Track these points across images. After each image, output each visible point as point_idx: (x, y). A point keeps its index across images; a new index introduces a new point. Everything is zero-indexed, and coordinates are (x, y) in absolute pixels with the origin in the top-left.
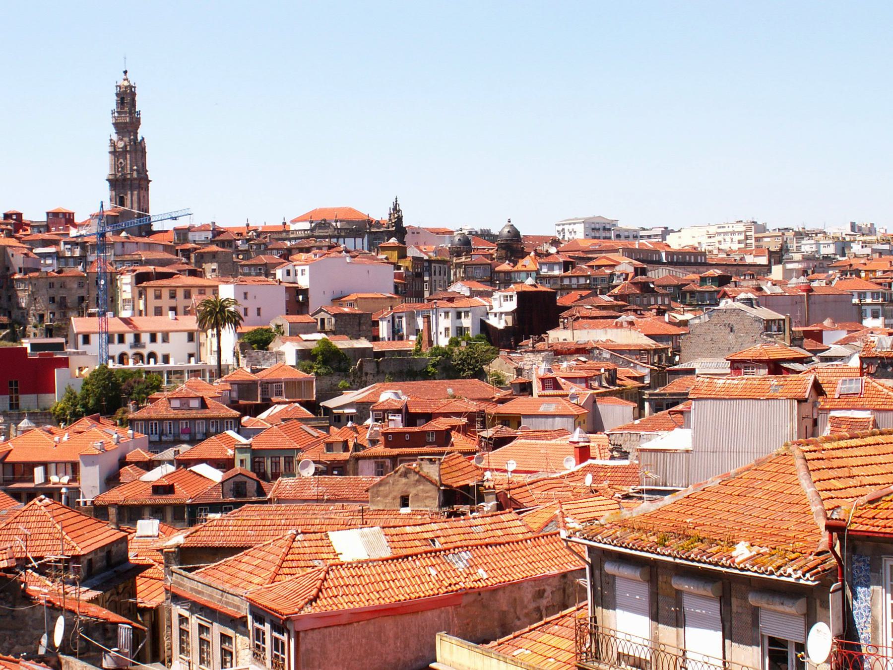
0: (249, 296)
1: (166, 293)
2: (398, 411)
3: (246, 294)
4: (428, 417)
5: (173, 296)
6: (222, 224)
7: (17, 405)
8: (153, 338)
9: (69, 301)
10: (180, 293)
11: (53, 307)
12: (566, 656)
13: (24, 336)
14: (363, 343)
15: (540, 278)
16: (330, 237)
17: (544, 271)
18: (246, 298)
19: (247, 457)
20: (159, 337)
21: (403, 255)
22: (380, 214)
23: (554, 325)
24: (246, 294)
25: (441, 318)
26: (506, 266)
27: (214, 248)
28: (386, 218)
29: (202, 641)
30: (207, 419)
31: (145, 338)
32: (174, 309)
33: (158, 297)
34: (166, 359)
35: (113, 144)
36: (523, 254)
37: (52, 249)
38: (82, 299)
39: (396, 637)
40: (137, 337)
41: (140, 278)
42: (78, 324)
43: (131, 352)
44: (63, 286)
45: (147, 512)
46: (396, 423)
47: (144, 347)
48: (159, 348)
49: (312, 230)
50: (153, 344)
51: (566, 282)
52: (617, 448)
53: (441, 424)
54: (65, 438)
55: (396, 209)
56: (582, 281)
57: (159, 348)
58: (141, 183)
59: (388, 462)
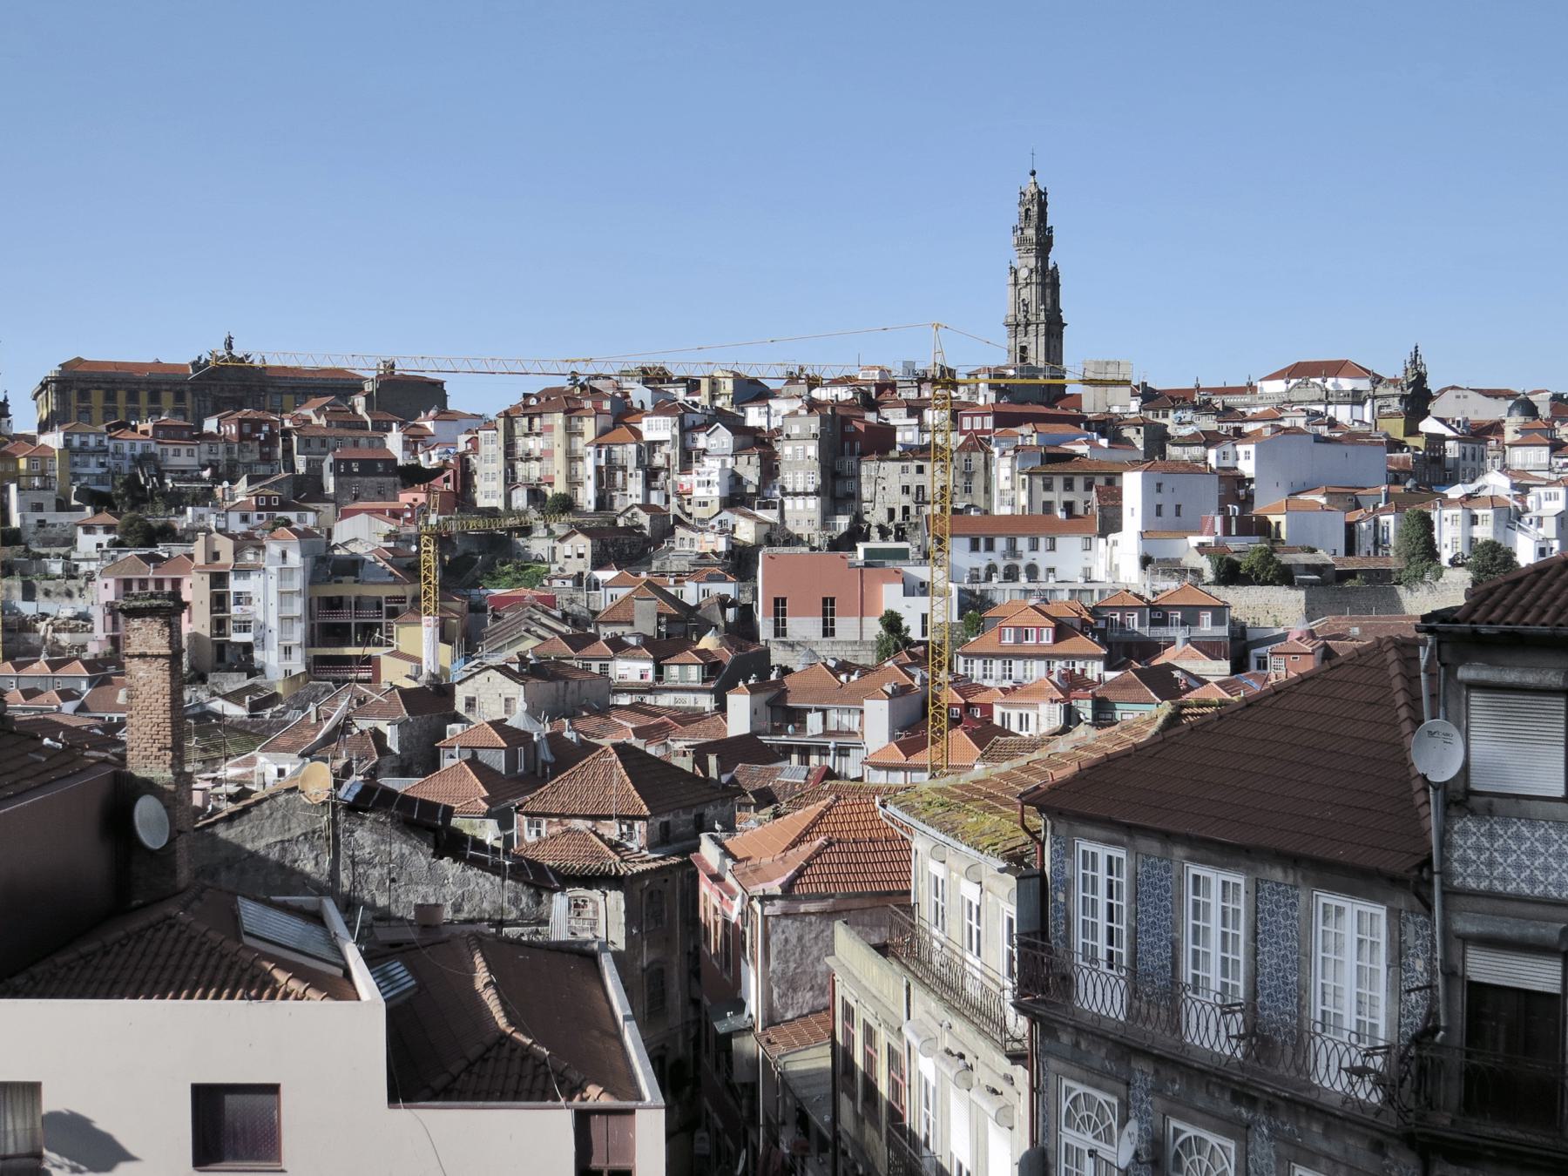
0: (1164, 488)
1: (1058, 482)
3: (1159, 485)
5: (1069, 486)
6: (1157, 384)
7: (833, 631)
8: (1034, 547)
9: (928, 491)
10: (1079, 483)
11: (907, 500)
13: (867, 538)
16: (1312, 402)
18: (1159, 491)
20: (1043, 542)
21: (1412, 431)
22: (1394, 367)
24: (1159, 485)
25: (1446, 525)
28: (1400, 375)
31: (1023, 544)
32: (1069, 507)
33: (1048, 487)
37: (915, 421)
43: (1001, 565)
44: (920, 470)
47: (1021, 557)
48: (1043, 559)
49: (1289, 391)
50: (1034, 554)
54: (854, 678)
58: (1055, 328)
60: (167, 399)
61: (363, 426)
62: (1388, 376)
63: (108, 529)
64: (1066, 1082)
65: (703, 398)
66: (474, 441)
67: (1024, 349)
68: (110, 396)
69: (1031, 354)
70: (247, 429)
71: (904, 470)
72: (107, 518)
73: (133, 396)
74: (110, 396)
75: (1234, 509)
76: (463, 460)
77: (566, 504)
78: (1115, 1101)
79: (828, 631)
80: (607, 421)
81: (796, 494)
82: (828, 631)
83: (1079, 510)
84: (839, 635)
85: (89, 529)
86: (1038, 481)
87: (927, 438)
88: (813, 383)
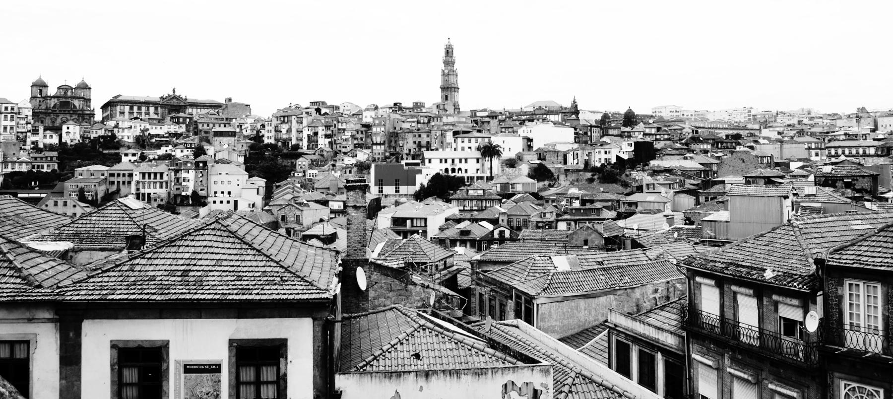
1: (466, 140)
2: (577, 199)
4: (592, 202)
5: (470, 141)
6: (494, 109)
8: (460, 161)
10: (473, 140)
11: (415, 146)
12: (675, 323)
13: (402, 159)
14: (560, 166)
15: (645, 134)
17: (647, 131)
19: (505, 218)
20: (463, 161)
22: (568, 104)
23: (654, 158)
26: (628, 129)
27: (487, 119)
29: (490, 306)
30: (486, 200)
31: (457, 161)
34: (466, 171)
35: (443, 71)
36: (636, 124)
38: (428, 142)
39: (585, 309)
40: (453, 160)
41: (456, 133)
42: (427, 154)
44: (420, 136)
45: (458, 244)
46: (577, 204)
48: (463, 166)
51: (658, 137)
52: (688, 219)
53: (598, 205)
55: (574, 102)
56: (666, 137)
57: (463, 166)
59: (573, 223)
60: (152, 109)
61: (222, 119)
62: (564, 106)
63: (134, 155)
64: (842, 383)
65: (341, 111)
66: (263, 126)
67: (446, 97)
68: (131, 108)
69: (449, 98)
70: (181, 120)
71: (415, 136)
72: (132, 151)
73: (139, 108)
74: (131, 108)
75: (526, 148)
76: (258, 132)
77: (297, 147)
78: (882, 391)
79: (397, 191)
80: (310, 118)
81: (377, 144)
82: (397, 191)
83: (473, 149)
84: (401, 193)
85: (126, 155)
86: (459, 140)
87: (419, 126)
88: (376, 108)
